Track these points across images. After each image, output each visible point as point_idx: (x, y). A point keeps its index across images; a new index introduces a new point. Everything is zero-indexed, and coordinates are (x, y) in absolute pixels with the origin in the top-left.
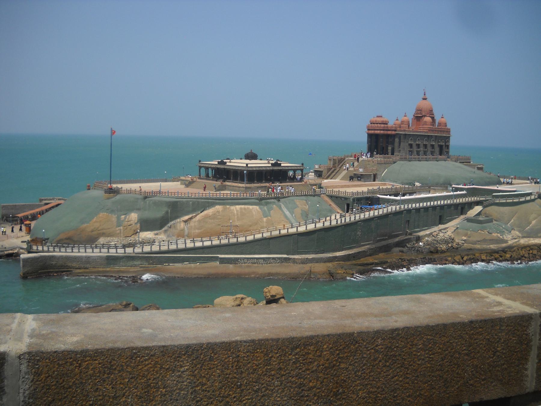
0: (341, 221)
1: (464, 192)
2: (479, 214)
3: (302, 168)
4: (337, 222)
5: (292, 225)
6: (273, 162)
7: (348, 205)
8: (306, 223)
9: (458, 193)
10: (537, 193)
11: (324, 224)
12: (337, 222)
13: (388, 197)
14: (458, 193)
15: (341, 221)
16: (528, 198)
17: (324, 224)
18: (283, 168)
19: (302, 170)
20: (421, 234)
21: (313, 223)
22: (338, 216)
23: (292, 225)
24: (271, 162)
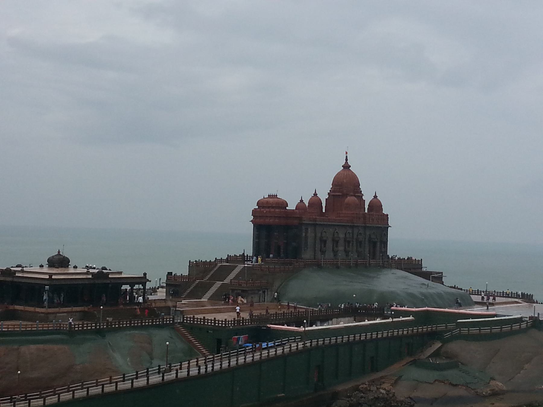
0: (206, 368)
1: (411, 318)
2: (436, 354)
3: (143, 281)
4: (199, 370)
5: (124, 377)
6: (96, 271)
7: (219, 342)
8: (148, 372)
9: (402, 319)
10: (531, 318)
11: (177, 373)
12: (199, 370)
13: (285, 327)
14: (402, 319)
15: (206, 368)
16: (516, 327)
17: (177, 373)
18: (113, 281)
19: (144, 285)
20: (340, 388)
21: (159, 373)
22: (201, 362)
23: (124, 377)
24: (91, 271)
